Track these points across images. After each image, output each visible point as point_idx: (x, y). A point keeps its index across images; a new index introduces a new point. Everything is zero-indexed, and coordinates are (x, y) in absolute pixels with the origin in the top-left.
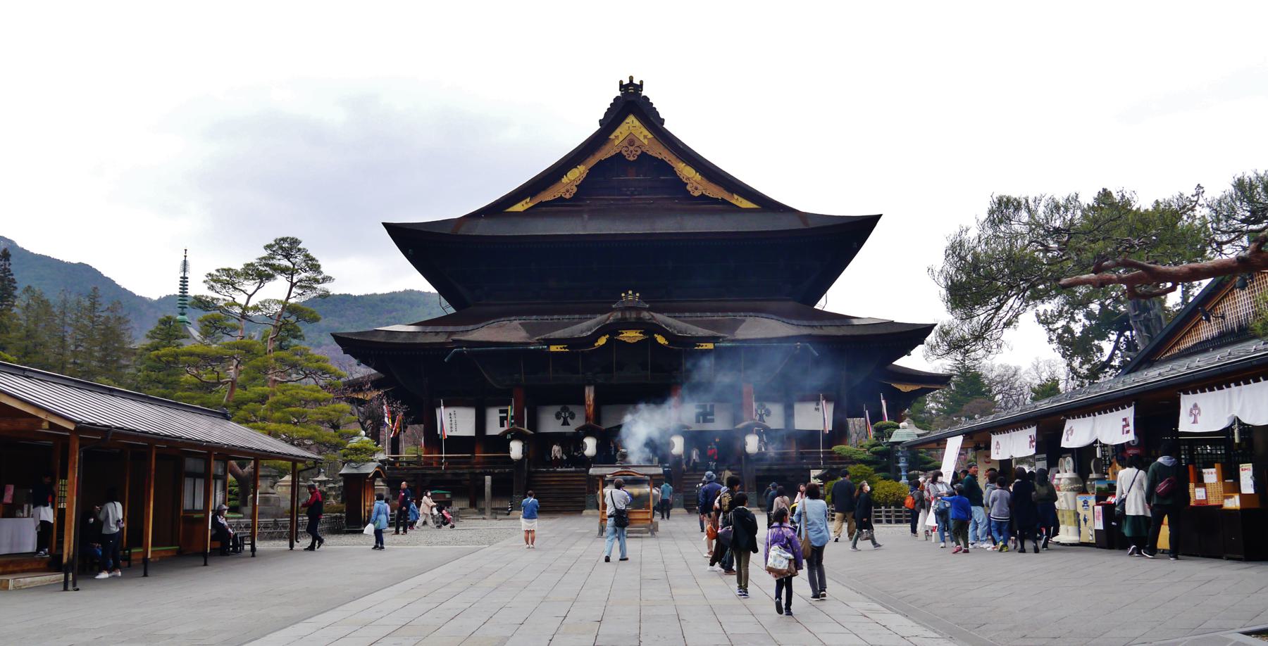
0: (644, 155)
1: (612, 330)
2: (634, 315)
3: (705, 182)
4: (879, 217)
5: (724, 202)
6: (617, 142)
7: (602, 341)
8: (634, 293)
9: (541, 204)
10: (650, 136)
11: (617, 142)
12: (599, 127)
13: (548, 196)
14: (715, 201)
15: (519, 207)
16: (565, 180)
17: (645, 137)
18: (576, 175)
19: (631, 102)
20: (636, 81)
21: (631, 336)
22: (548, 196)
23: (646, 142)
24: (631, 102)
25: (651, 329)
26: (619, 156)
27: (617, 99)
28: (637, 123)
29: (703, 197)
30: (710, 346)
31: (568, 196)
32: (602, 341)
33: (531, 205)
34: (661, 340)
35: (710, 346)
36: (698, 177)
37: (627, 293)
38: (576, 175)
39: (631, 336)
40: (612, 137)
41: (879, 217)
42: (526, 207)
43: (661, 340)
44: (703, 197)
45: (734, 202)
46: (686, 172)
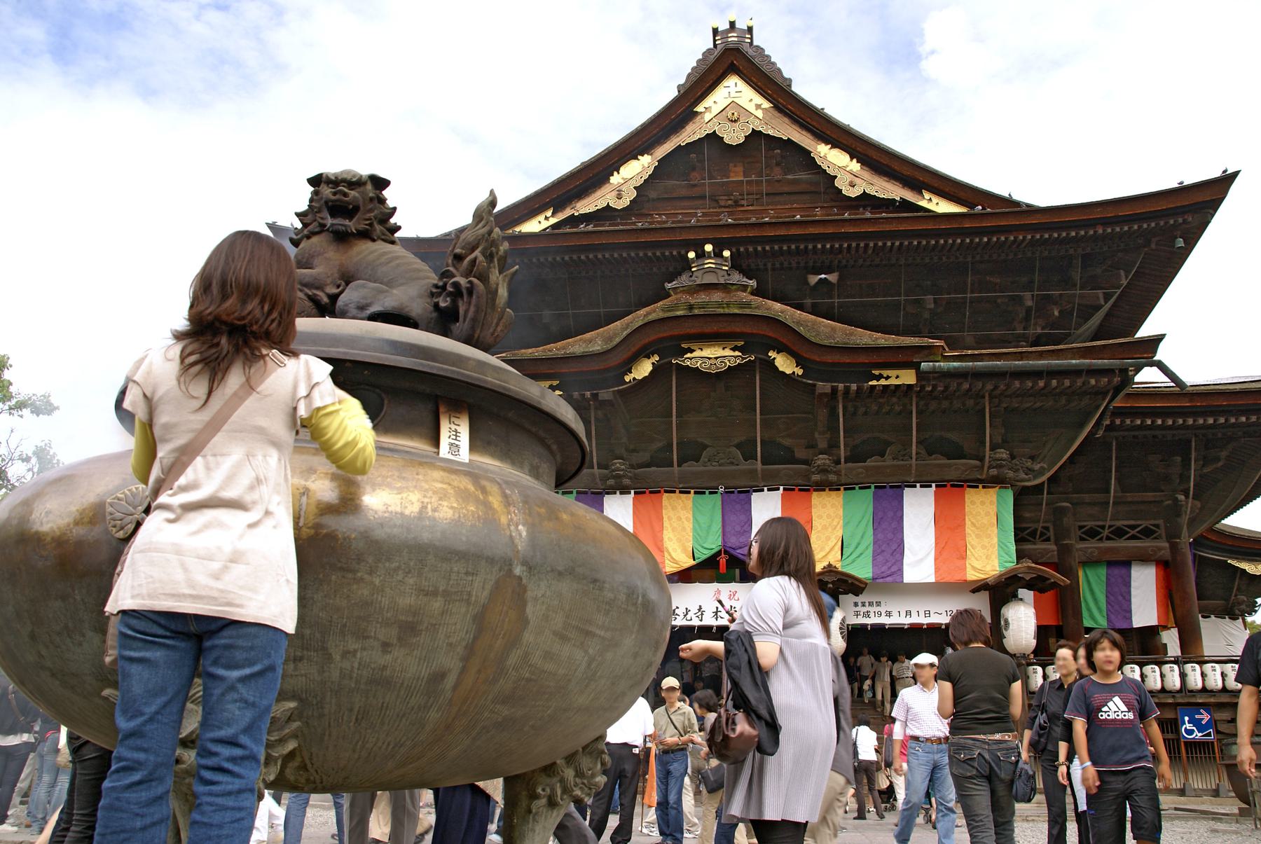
0: (756, 134)
1: (668, 341)
2: (717, 296)
3: (867, 175)
4: (1227, 180)
5: (906, 205)
6: (707, 117)
7: (644, 369)
8: (718, 254)
9: (573, 220)
10: (766, 105)
11: (707, 117)
12: (674, 93)
13: (585, 206)
14: (888, 204)
15: (534, 226)
16: (615, 179)
17: (758, 107)
18: (636, 170)
19: (733, 58)
20: (741, 25)
21: (712, 356)
22: (585, 206)
23: (760, 114)
24: (733, 58)
25: (758, 337)
26: (713, 138)
27: (707, 53)
28: (742, 85)
29: (865, 195)
30: (907, 377)
31: (620, 205)
32: (644, 369)
33: (553, 221)
34: (784, 364)
35: (907, 377)
36: (855, 166)
37: (701, 255)
38: (636, 170)
39: (712, 356)
40: (699, 109)
41: (1227, 180)
42: (545, 224)
43: (784, 364)
44: (866, 199)
45: (923, 203)
46: (833, 158)
